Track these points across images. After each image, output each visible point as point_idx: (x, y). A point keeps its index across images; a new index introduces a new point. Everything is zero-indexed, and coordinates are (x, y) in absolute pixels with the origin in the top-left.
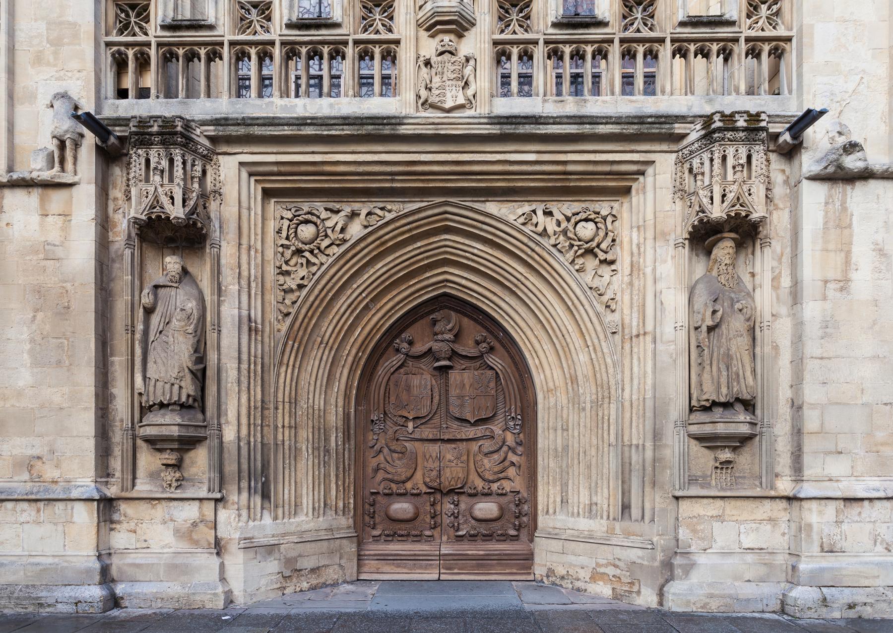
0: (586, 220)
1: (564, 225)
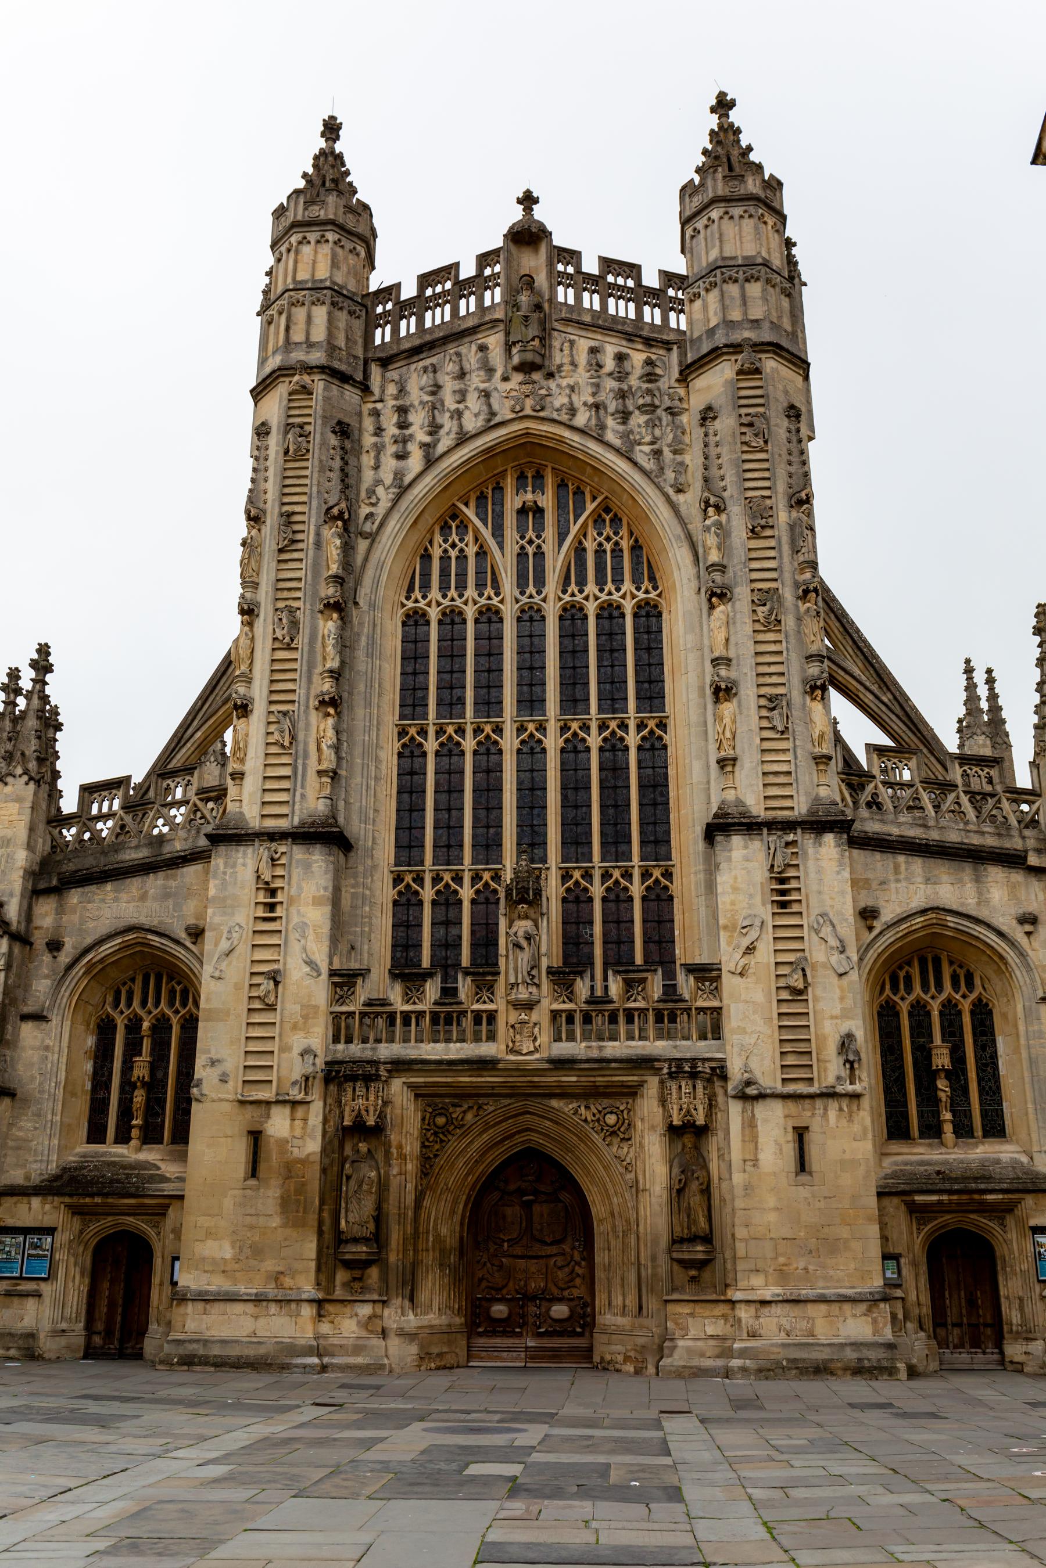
0: (611, 1113)
1: (598, 1116)
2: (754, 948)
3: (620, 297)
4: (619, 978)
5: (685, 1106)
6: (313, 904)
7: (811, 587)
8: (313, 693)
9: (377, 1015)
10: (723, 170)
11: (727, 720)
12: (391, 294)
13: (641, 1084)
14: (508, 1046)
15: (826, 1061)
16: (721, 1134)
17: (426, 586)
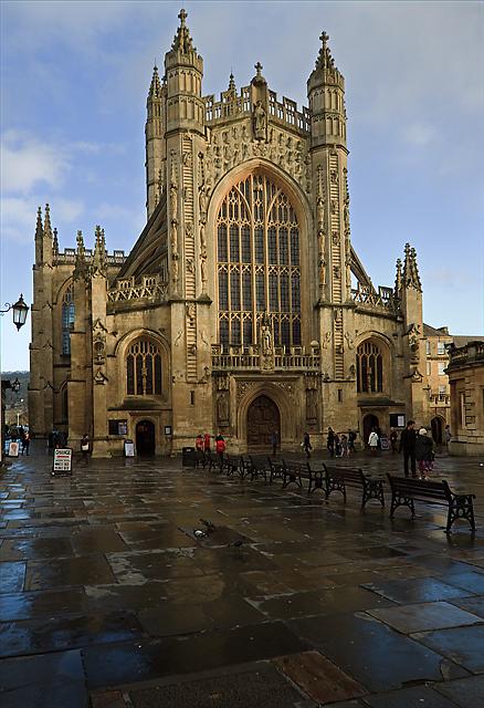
17: (225, 215)
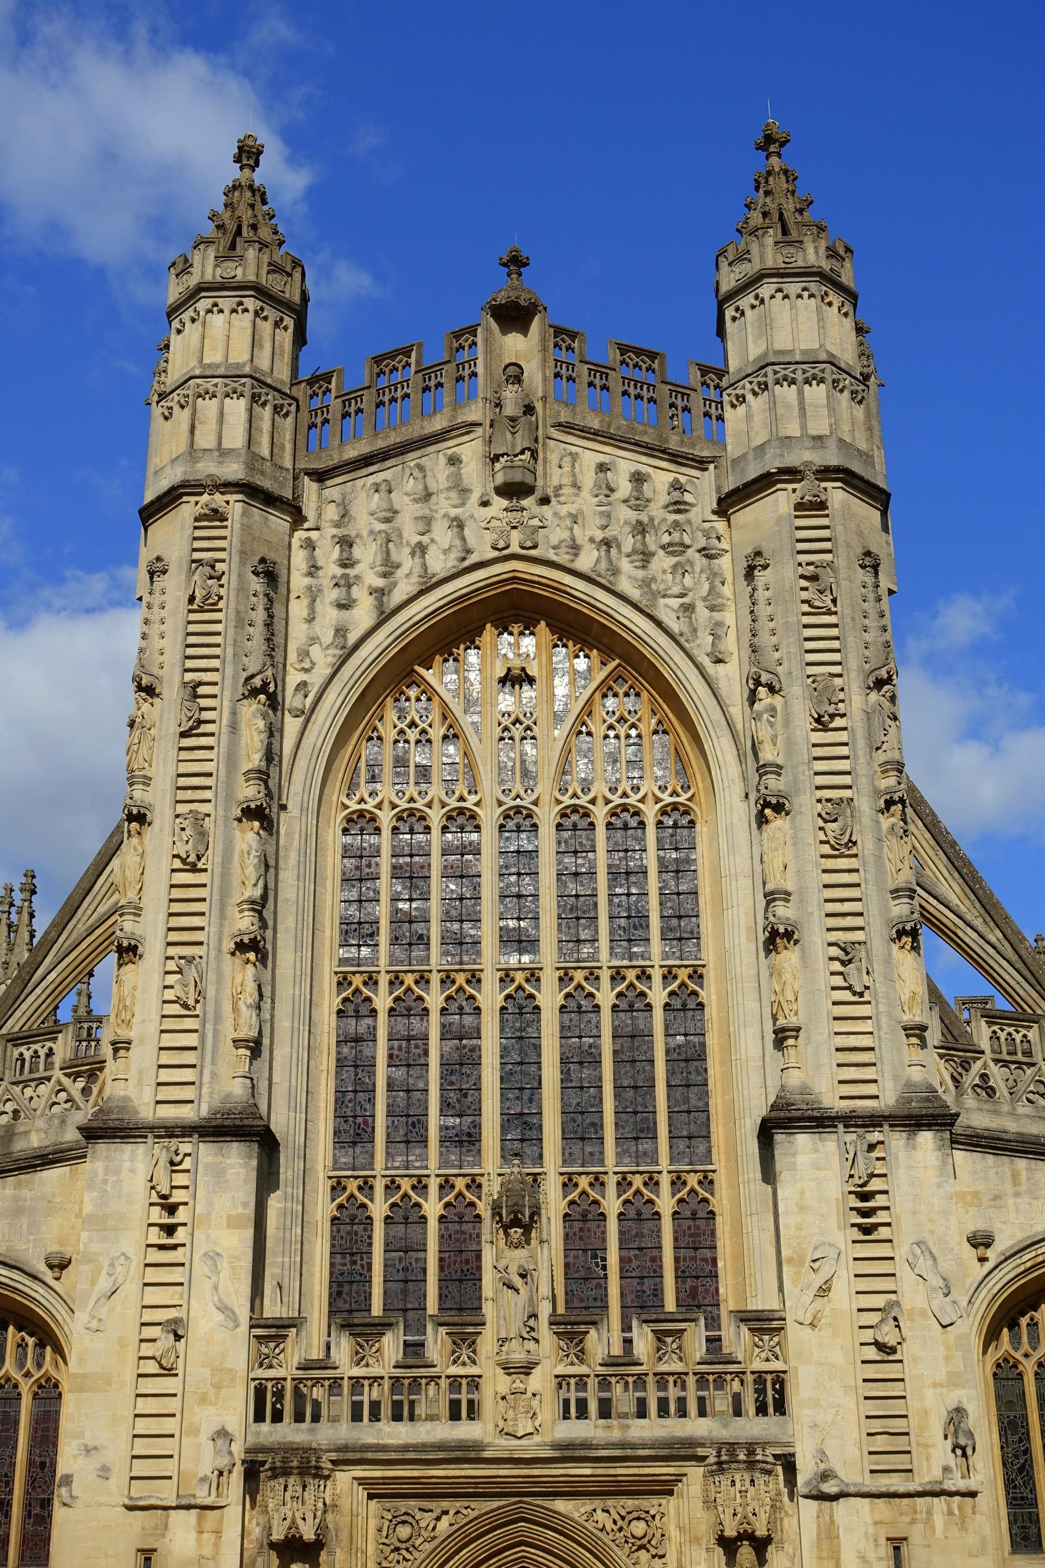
0: (638, 1519)
1: (620, 1523)
2: (829, 1289)
3: (638, 397)
4: (647, 1329)
5: (739, 1509)
6: (229, 1226)
7: (896, 798)
8: (227, 932)
9: (317, 1381)
10: (776, 235)
11: (787, 976)
12: (330, 383)
13: (679, 1478)
14: (497, 1426)
15: (928, 1446)
16: (789, 1548)
